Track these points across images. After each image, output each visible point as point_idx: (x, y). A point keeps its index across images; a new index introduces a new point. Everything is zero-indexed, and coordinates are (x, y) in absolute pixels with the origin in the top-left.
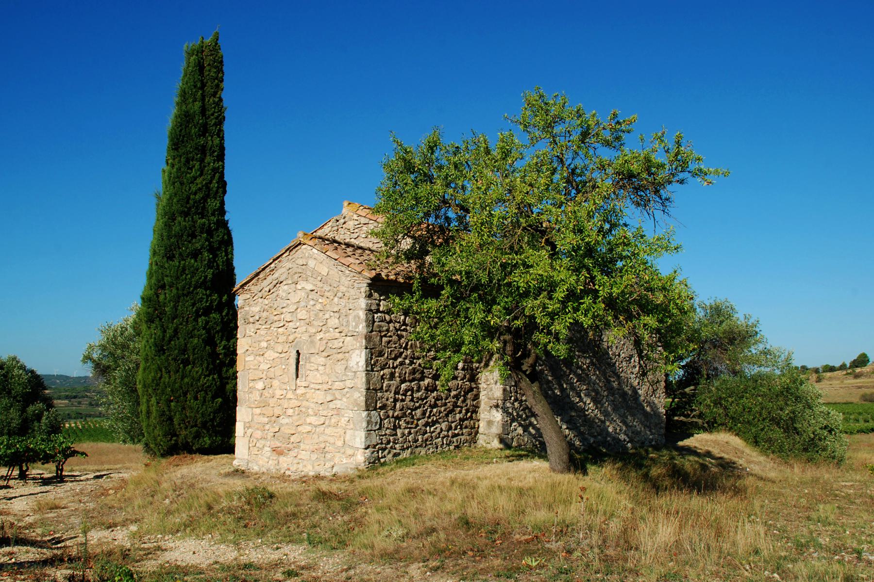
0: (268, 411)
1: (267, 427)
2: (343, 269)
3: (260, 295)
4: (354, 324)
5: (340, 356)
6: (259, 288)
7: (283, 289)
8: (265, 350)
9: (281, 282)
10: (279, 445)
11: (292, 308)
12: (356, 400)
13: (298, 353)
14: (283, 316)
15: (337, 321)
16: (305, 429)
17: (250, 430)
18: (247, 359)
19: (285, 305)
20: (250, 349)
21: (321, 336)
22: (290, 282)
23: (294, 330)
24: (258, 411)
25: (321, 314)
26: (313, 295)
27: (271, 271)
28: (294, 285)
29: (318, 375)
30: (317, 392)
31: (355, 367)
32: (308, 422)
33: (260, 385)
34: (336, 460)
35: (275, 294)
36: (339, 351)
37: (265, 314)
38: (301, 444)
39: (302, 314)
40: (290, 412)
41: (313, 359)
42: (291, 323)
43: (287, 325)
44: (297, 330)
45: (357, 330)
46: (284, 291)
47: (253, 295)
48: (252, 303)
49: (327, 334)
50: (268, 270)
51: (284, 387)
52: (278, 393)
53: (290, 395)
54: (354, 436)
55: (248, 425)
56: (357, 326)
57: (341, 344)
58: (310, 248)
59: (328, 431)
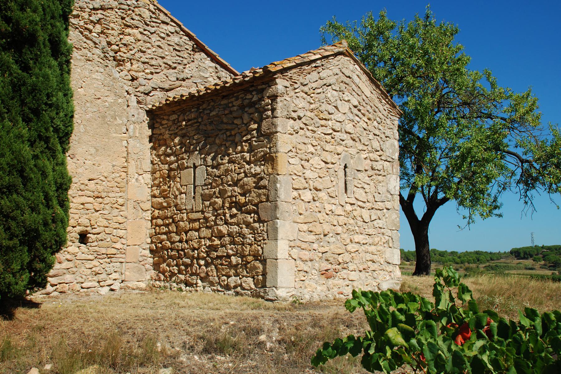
0: (318, 229)
1: (315, 246)
2: (380, 97)
3: (306, 89)
4: (391, 151)
5: (380, 178)
6: (301, 79)
7: (330, 93)
8: (311, 155)
9: (330, 85)
10: (329, 266)
11: (340, 117)
12: (393, 220)
13: (346, 167)
14: (330, 123)
15: (378, 144)
16: (353, 248)
17: (294, 250)
18: (292, 161)
19: (333, 112)
20: (294, 150)
21: (367, 155)
22: (338, 89)
23: (341, 142)
24: (305, 227)
25: (365, 132)
26: (355, 111)
27: (315, 67)
28: (341, 93)
29: (364, 194)
30: (362, 210)
31: (393, 190)
32: (357, 241)
33: (307, 195)
34: (380, 277)
35: (322, 95)
36: (380, 173)
37: (309, 114)
38: (350, 264)
39: (349, 127)
40: (339, 229)
41: (360, 175)
42: (338, 133)
43: (335, 133)
44: (344, 143)
45: (394, 157)
46: (332, 96)
47: (296, 86)
48: (292, 93)
49: (371, 155)
50: (314, 65)
51: (333, 201)
52: (328, 207)
53: (339, 211)
54: (393, 253)
55: (292, 244)
56: (393, 153)
57: (381, 167)
58: (352, 62)
59: (372, 248)
